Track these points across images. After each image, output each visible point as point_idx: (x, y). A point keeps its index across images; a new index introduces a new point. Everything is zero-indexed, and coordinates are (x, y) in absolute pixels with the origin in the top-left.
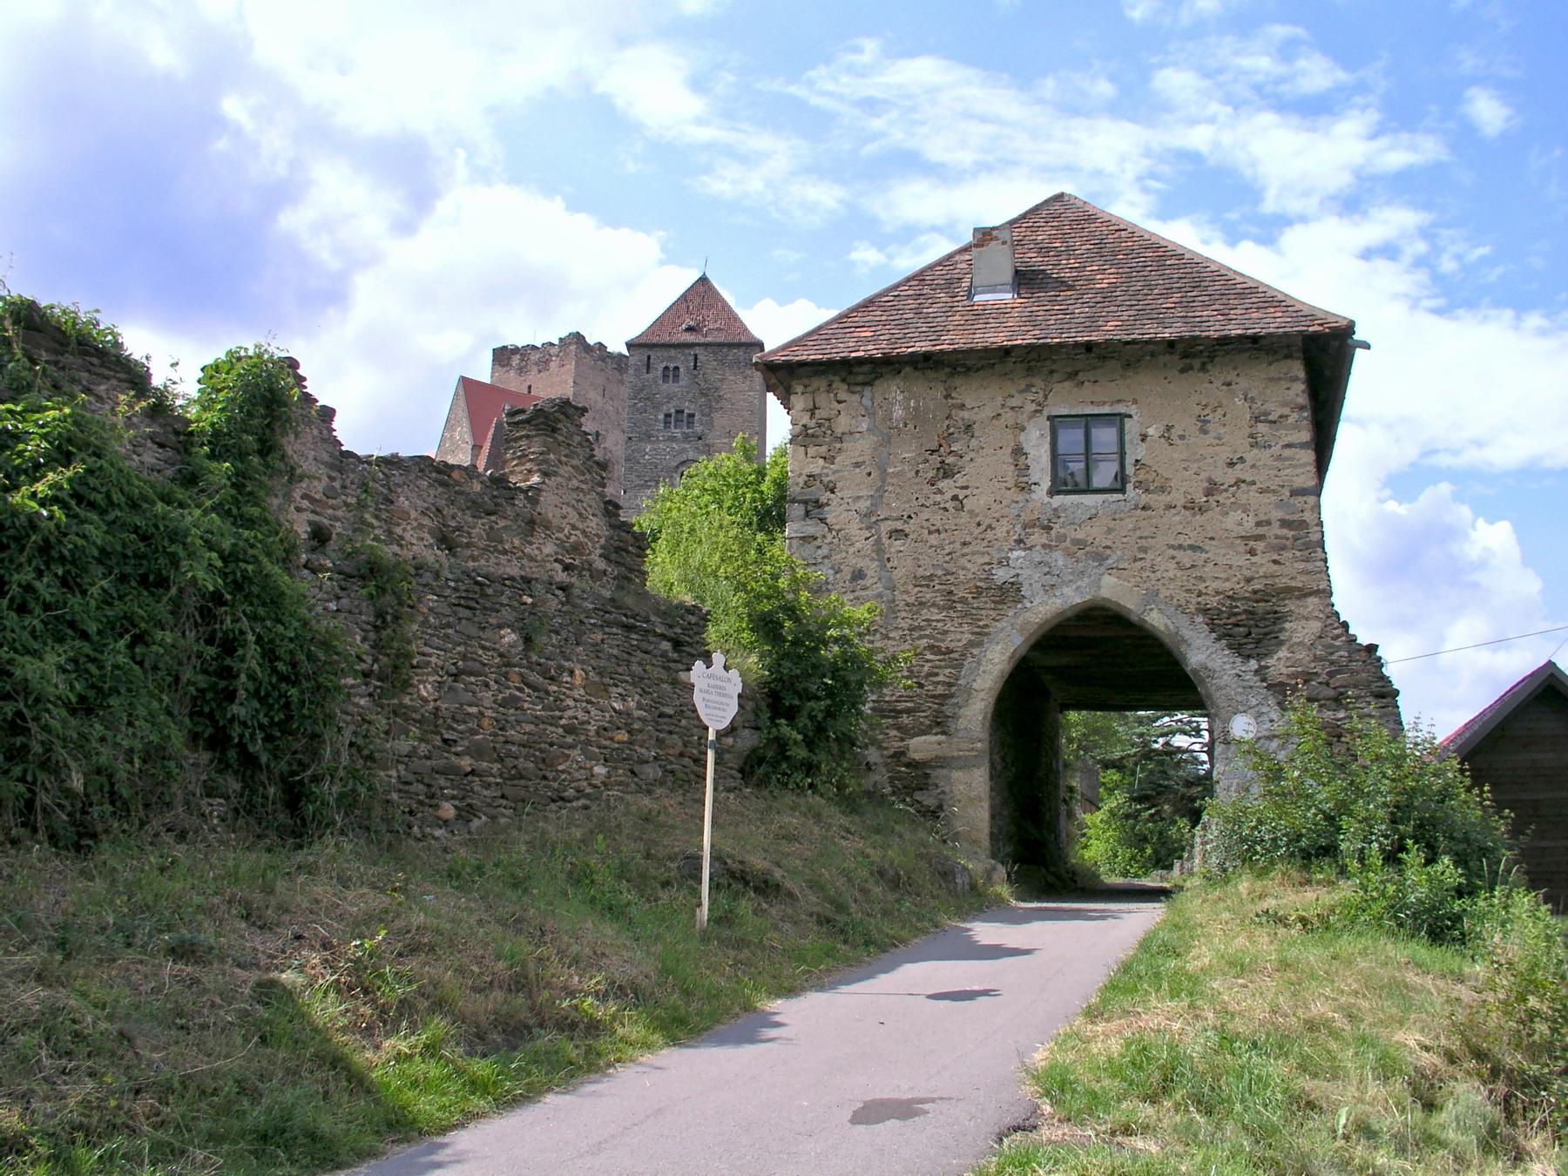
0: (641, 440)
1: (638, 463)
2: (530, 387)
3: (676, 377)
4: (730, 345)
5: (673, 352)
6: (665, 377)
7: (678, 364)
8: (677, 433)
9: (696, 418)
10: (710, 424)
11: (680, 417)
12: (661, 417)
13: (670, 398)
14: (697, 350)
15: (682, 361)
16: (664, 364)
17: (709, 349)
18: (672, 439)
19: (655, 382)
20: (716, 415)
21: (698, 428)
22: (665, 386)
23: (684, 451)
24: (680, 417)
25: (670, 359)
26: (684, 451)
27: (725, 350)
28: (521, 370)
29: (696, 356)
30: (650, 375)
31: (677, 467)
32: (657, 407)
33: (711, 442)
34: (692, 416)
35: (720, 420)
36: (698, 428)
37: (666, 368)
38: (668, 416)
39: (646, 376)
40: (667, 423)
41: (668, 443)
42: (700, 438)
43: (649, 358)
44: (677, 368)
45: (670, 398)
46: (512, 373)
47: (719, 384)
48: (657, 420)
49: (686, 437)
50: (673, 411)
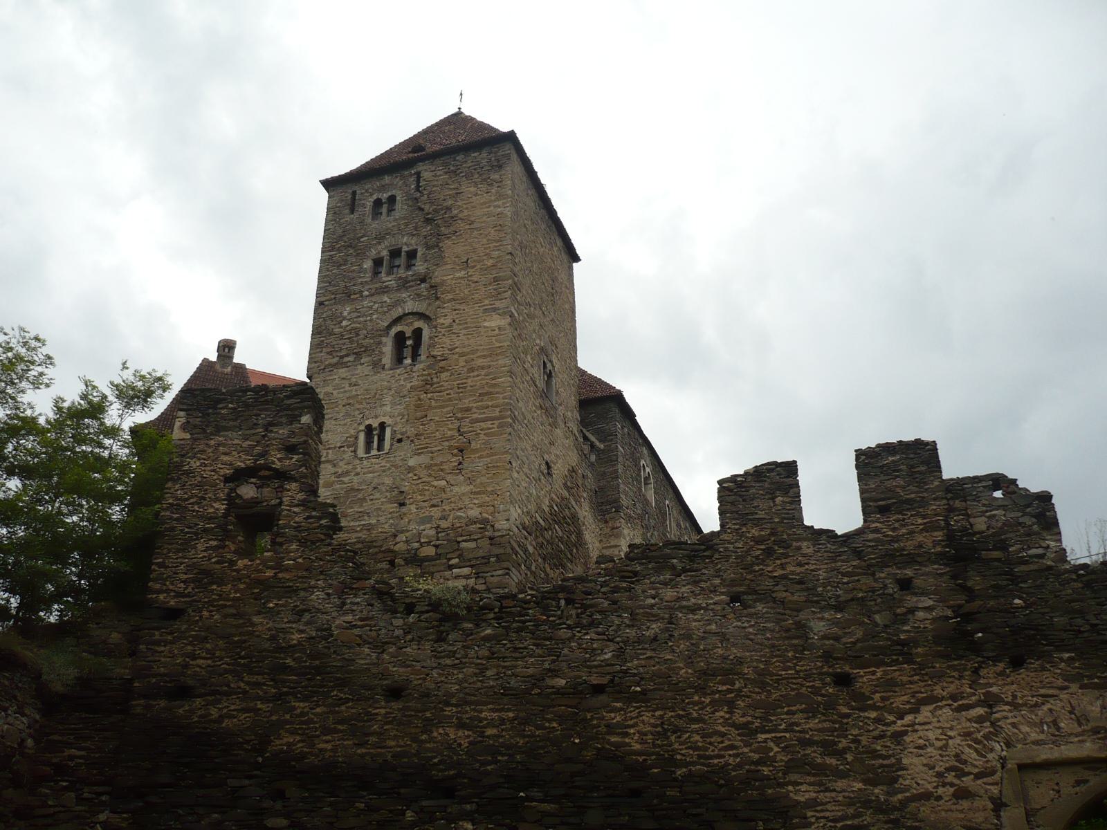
0: (336, 301)
1: (331, 334)
4: (467, 148)
5: (387, 179)
6: (376, 212)
7: (394, 192)
8: (389, 280)
9: (419, 254)
12: (368, 264)
13: (381, 238)
14: (421, 167)
15: (398, 187)
16: (375, 197)
17: (438, 162)
18: (385, 290)
19: (362, 222)
21: (420, 267)
23: (399, 302)
25: (383, 188)
27: (460, 157)
29: (418, 174)
30: (356, 215)
31: (389, 327)
32: (361, 255)
33: (438, 280)
34: (412, 255)
35: (454, 249)
37: (378, 203)
38: (378, 262)
39: (349, 218)
40: (376, 273)
41: (376, 298)
42: (423, 280)
43: (354, 193)
44: (392, 200)
45: (381, 238)
47: (450, 202)
48: (361, 270)
49: (404, 284)
50: (385, 253)
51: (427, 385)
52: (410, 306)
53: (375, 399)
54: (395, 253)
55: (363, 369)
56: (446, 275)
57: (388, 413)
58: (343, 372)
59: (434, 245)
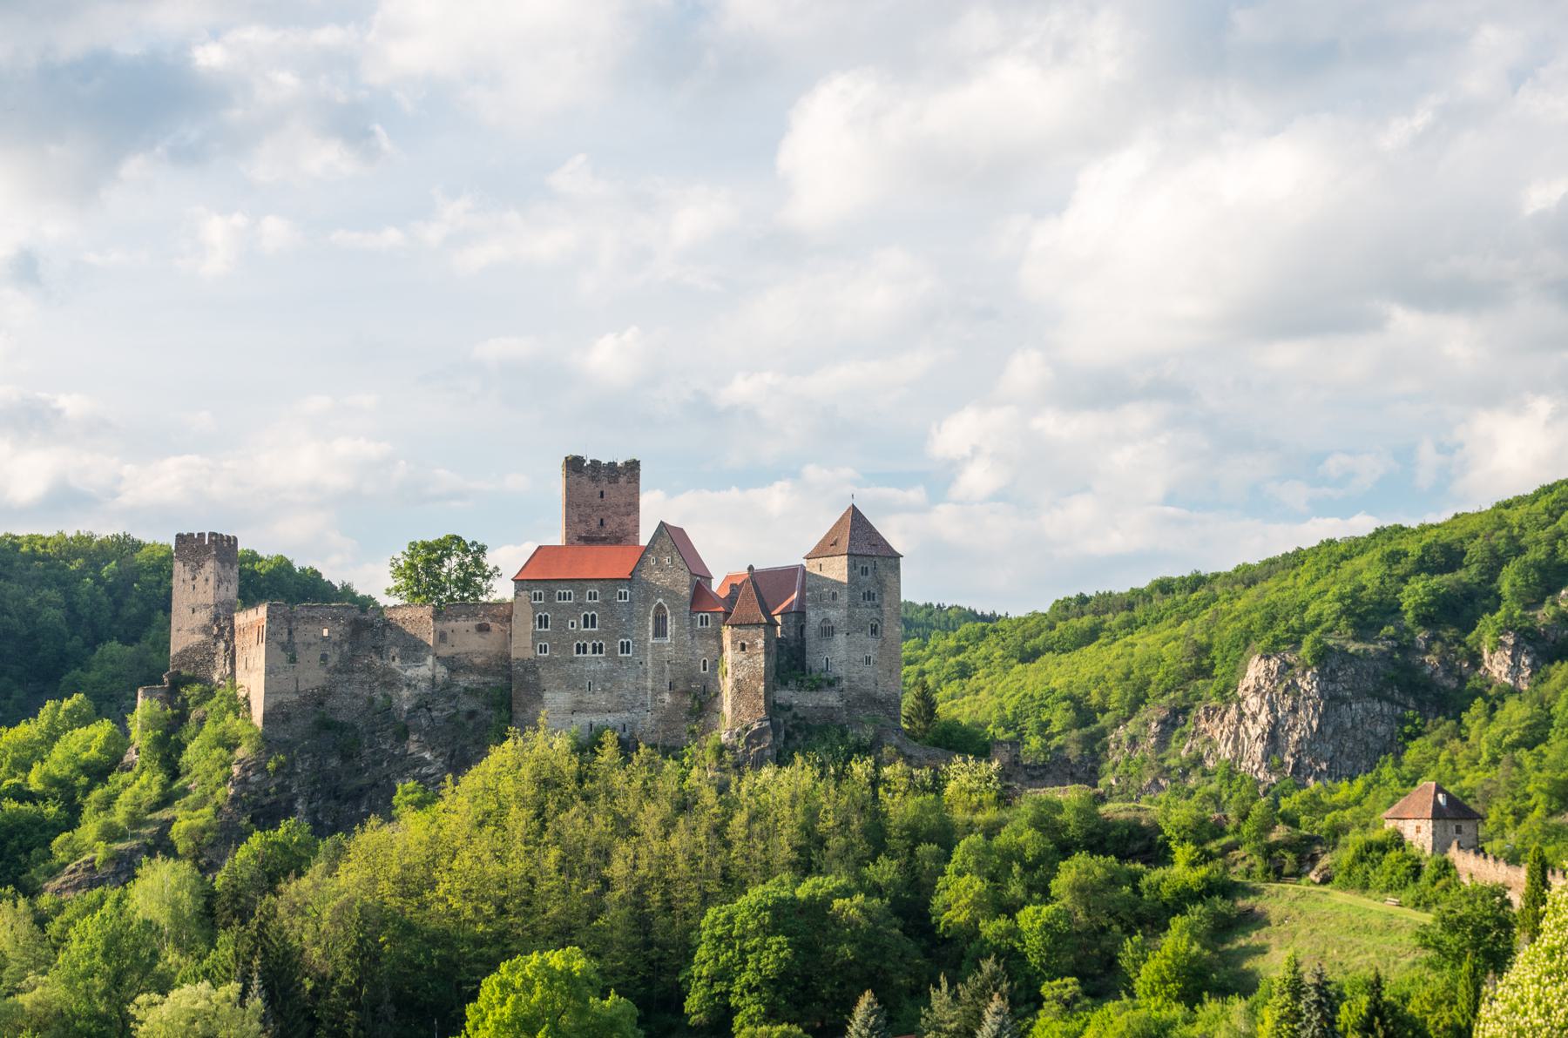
2: (602, 493)
3: (867, 574)
8: (868, 603)
10: (882, 599)
11: (869, 596)
14: (876, 559)
18: (867, 606)
20: (884, 595)
21: (877, 601)
22: (862, 578)
24: (869, 596)
25: (864, 563)
26: (871, 613)
28: (593, 479)
32: (860, 589)
35: (886, 598)
36: (877, 601)
46: (585, 480)
49: (872, 606)
51: (882, 646)
52: (875, 615)
53: (867, 647)
54: (869, 592)
55: (863, 635)
56: (886, 608)
57: (871, 653)
58: (857, 634)
59: (881, 592)
